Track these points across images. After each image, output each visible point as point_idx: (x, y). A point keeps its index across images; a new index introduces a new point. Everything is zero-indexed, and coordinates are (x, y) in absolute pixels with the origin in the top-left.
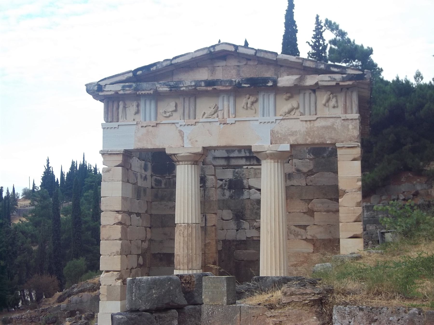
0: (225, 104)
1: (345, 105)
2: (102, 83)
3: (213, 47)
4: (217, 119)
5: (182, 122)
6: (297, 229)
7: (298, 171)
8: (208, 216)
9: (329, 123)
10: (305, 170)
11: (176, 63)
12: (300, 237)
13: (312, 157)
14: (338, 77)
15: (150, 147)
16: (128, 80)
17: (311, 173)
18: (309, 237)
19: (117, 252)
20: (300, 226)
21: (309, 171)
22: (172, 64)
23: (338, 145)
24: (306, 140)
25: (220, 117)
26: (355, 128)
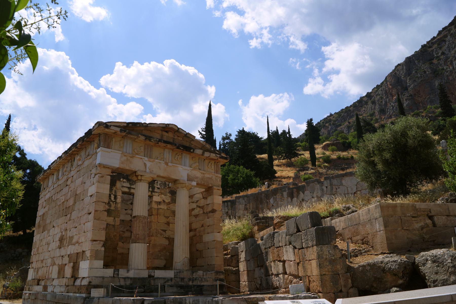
0: (168, 154)
2: (109, 124)
4: (164, 162)
5: (146, 159)
6: (162, 232)
7: (164, 201)
9: (210, 176)
10: (167, 201)
13: (170, 195)
14: (218, 156)
15: (127, 168)
16: (124, 127)
17: (169, 203)
18: (167, 237)
19: (104, 229)
20: (163, 230)
23: (215, 187)
25: (165, 160)
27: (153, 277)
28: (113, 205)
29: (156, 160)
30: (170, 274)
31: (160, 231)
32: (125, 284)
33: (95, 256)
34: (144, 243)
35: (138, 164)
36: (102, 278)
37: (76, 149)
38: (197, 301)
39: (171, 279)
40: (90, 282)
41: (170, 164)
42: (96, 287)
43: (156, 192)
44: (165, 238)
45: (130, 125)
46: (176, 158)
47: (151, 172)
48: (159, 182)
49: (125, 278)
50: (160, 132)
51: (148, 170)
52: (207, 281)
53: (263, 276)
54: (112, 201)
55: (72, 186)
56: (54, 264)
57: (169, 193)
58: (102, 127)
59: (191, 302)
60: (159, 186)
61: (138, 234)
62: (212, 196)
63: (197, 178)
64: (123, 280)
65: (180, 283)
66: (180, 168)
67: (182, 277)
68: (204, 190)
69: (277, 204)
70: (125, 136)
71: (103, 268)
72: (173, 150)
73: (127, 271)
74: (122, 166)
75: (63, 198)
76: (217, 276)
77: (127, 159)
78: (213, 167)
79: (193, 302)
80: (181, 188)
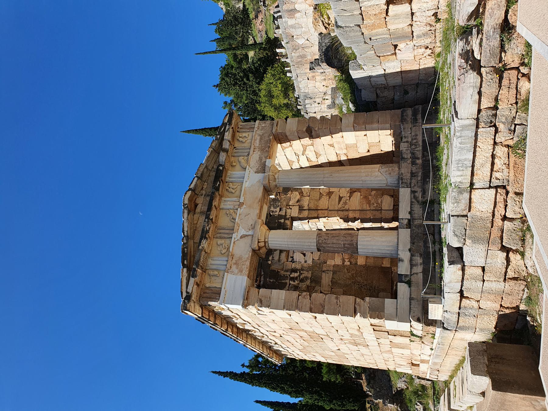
1: (248, 129)
2: (184, 294)
3: (184, 205)
4: (239, 209)
5: (234, 236)
6: (341, 203)
7: (298, 201)
8: (324, 269)
9: (259, 138)
10: (298, 197)
11: (187, 233)
12: (347, 201)
13: (290, 193)
14: (227, 127)
15: (248, 263)
18: (348, 195)
19: (337, 298)
21: (300, 194)
22: (187, 237)
24: (266, 151)
25: (237, 207)
26: (265, 123)
27: (409, 220)
28: (305, 274)
29: (237, 220)
30: (405, 194)
31: (340, 206)
32: (421, 264)
33: (377, 312)
34: (358, 235)
35: (242, 249)
36: (412, 301)
37: (229, 330)
38: (458, 164)
39: (413, 192)
40: (418, 320)
41: (242, 201)
42: (425, 311)
43: (286, 212)
44: (350, 197)
45: (185, 263)
46: (233, 191)
47: (253, 227)
48: (272, 209)
49: (412, 265)
50: (196, 216)
51: (250, 233)
52: (416, 135)
53: (411, 44)
54: (300, 276)
55: (281, 332)
56: (390, 352)
57: (286, 194)
58: (188, 305)
59: (460, 173)
60: (278, 209)
61: (344, 244)
62: (288, 134)
63: (260, 159)
64: (414, 267)
65: (419, 178)
66: (246, 185)
67: (409, 175)
68: (279, 145)
69: (305, 32)
70: (202, 268)
71: (396, 298)
72: (221, 196)
73: (401, 262)
74: (246, 271)
75: (298, 340)
76: (409, 119)
77: (235, 264)
78: (244, 135)
79: (459, 170)
80: (275, 181)
